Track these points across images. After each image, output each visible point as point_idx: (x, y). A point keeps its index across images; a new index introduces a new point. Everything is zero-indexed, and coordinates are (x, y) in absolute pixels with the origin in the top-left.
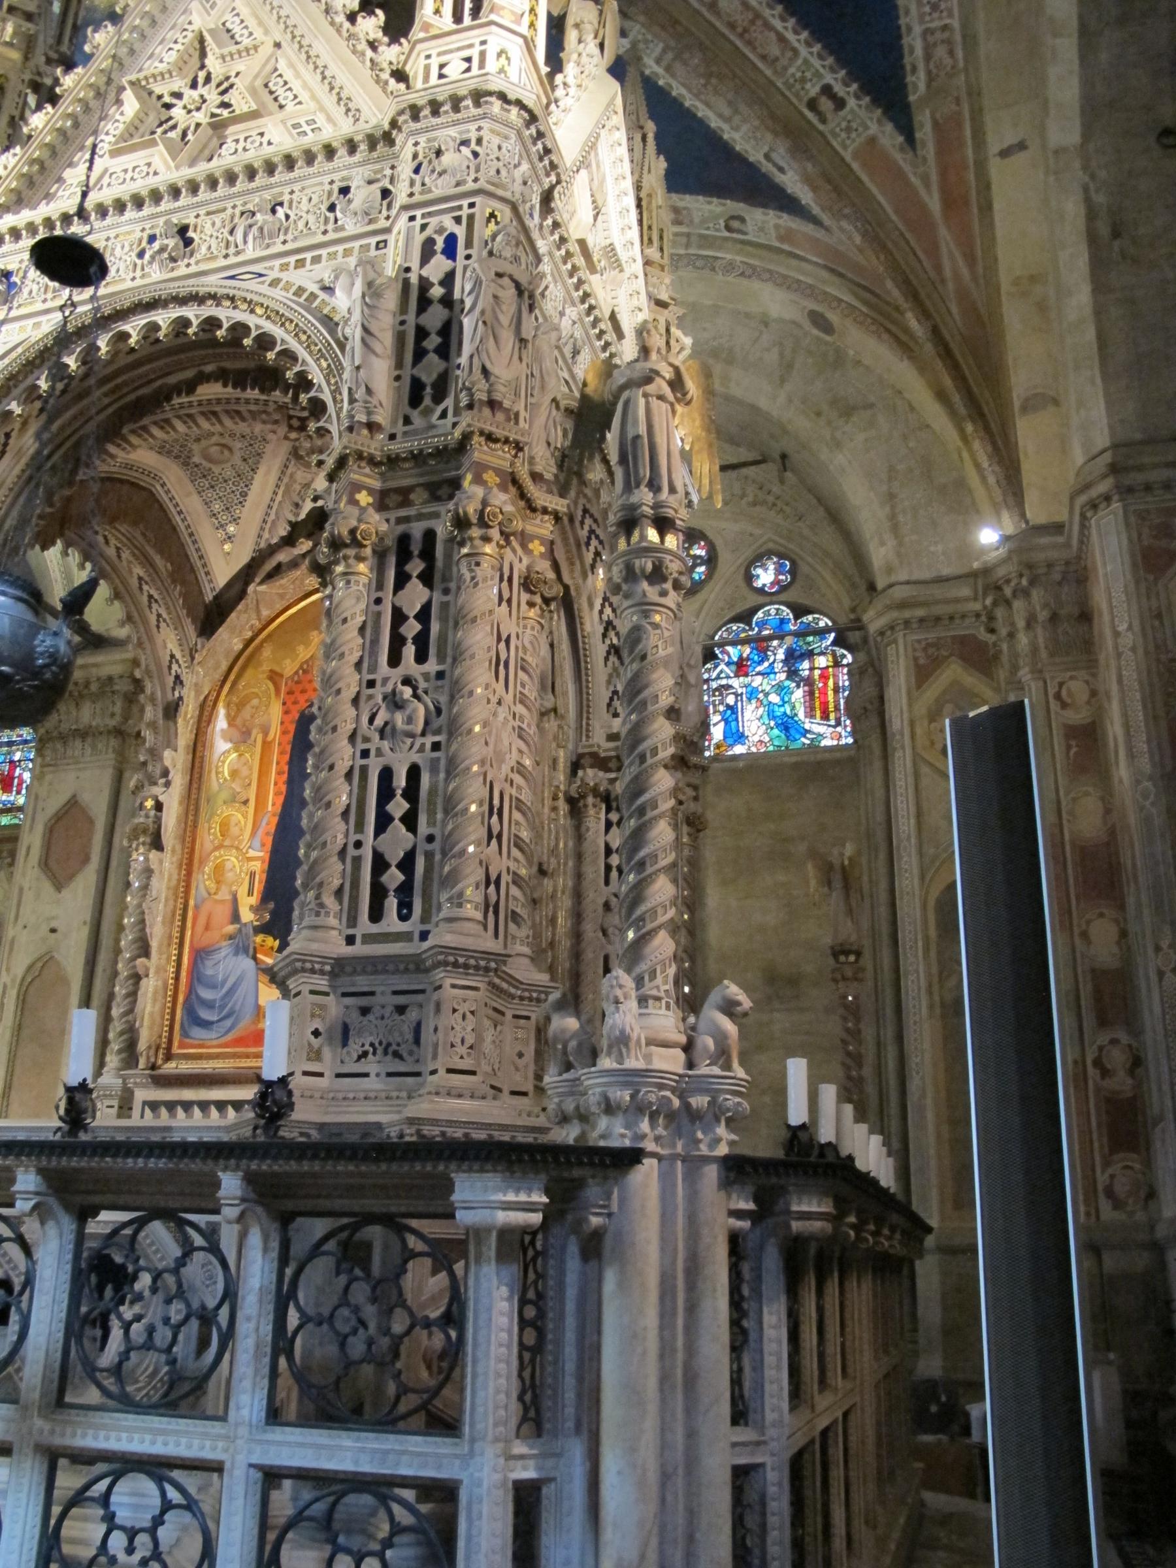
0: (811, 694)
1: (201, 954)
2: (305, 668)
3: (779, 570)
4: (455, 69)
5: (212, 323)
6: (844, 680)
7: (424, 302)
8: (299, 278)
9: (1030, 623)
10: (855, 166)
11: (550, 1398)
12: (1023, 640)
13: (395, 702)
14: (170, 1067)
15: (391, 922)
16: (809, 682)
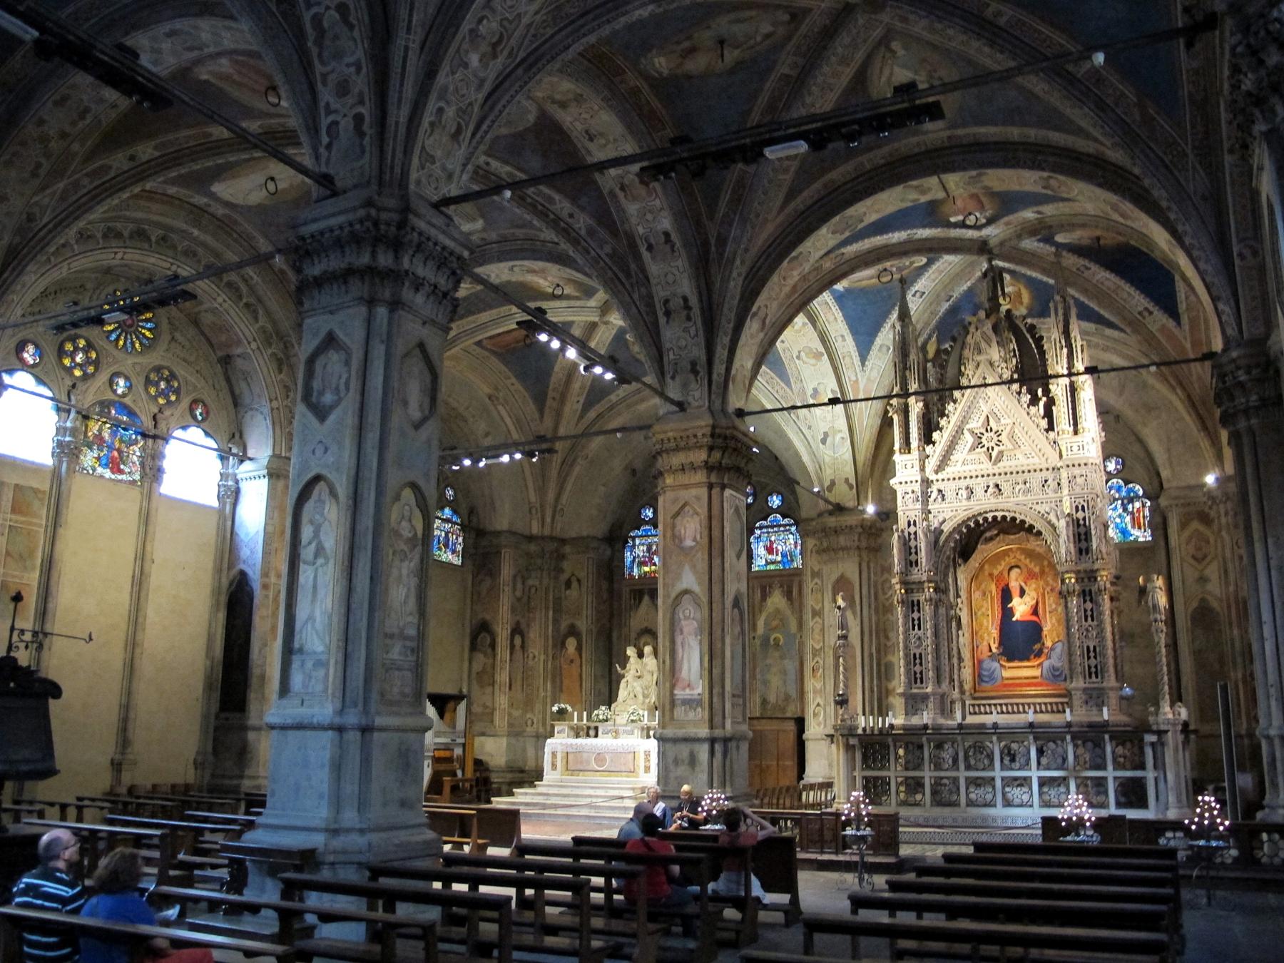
0: (1133, 519)
1: (980, 662)
2: (1001, 573)
3: (1117, 463)
4: (1075, 448)
5: (1014, 519)
6: (1147, 513)
7: (1079, 525)
8: (1038, 508)
9: (1226, 514)
10: (1157, 334)
11: (1159, 765)
12: (1223, 520)
13: (1087, 630)
14: (977, 695)
15: (1094, 678)
16: (1132, 513)
